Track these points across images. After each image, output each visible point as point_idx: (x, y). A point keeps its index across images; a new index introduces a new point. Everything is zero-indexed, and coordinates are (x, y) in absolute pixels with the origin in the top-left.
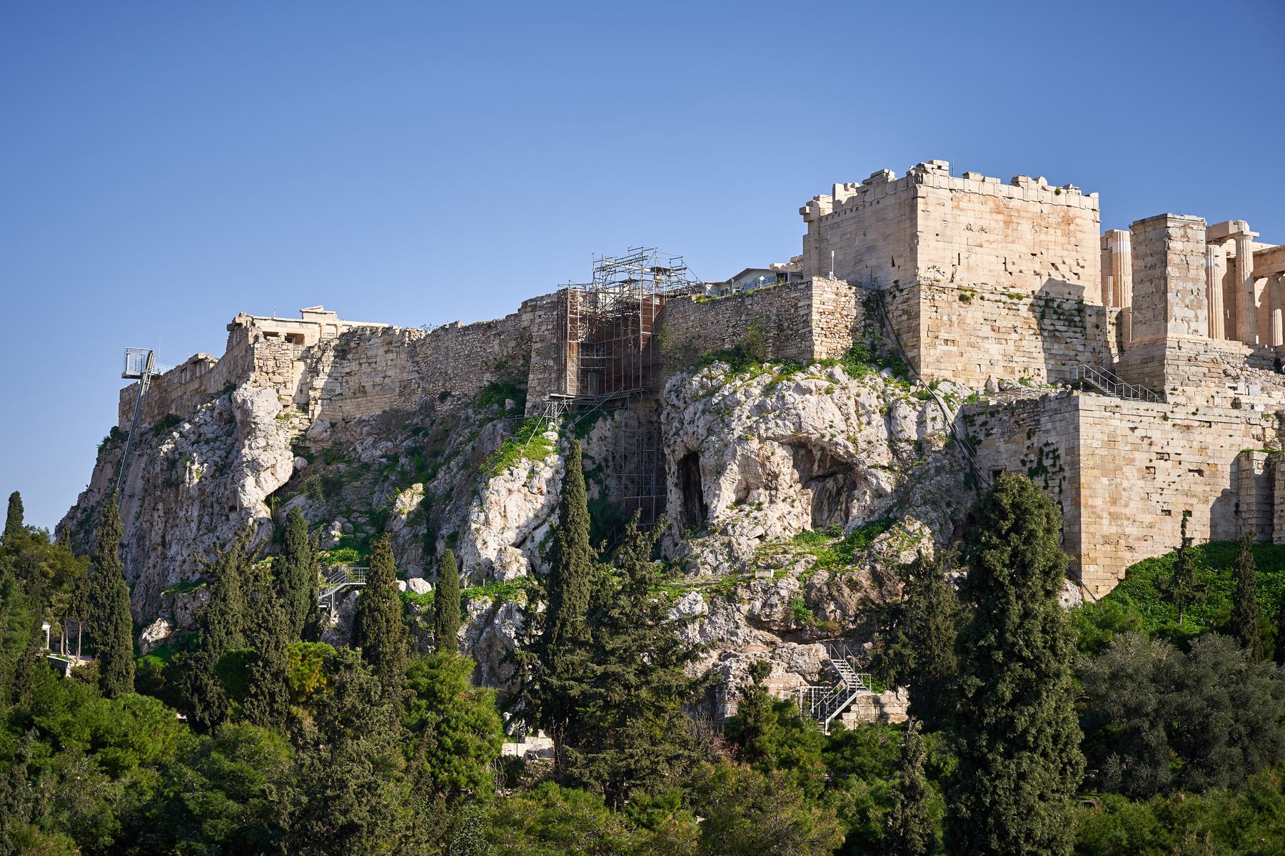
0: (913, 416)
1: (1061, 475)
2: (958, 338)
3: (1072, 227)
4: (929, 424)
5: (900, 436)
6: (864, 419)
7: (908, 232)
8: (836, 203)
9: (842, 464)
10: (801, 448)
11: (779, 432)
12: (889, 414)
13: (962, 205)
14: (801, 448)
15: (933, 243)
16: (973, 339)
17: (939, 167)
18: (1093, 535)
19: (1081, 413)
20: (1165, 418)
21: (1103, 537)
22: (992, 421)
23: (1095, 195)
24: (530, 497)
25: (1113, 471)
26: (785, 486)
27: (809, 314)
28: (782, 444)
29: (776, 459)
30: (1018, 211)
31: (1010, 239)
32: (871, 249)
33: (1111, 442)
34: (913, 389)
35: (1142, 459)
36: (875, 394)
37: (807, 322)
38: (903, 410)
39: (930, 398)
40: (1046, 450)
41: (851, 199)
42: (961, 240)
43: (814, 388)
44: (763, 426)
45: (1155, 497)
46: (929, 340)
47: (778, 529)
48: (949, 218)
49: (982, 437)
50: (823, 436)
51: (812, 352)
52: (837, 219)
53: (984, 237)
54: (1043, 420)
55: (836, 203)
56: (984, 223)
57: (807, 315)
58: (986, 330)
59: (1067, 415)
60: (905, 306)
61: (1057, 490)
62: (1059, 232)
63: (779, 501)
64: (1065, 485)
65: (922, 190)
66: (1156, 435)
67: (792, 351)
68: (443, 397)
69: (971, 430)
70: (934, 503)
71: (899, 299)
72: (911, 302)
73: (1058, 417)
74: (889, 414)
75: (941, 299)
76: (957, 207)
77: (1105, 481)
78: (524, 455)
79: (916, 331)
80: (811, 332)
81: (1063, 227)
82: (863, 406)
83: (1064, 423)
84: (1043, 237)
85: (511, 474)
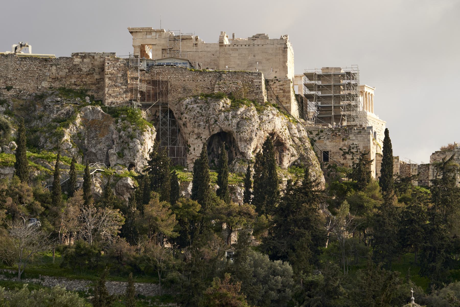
5: (295, 135)
7: (282, 60)
22: (321, 134)
40: (352, 146)
49: (316, 139)
59: (364, 135)
60: (281, 87)
73: (359, 136)
83: (361, 138)
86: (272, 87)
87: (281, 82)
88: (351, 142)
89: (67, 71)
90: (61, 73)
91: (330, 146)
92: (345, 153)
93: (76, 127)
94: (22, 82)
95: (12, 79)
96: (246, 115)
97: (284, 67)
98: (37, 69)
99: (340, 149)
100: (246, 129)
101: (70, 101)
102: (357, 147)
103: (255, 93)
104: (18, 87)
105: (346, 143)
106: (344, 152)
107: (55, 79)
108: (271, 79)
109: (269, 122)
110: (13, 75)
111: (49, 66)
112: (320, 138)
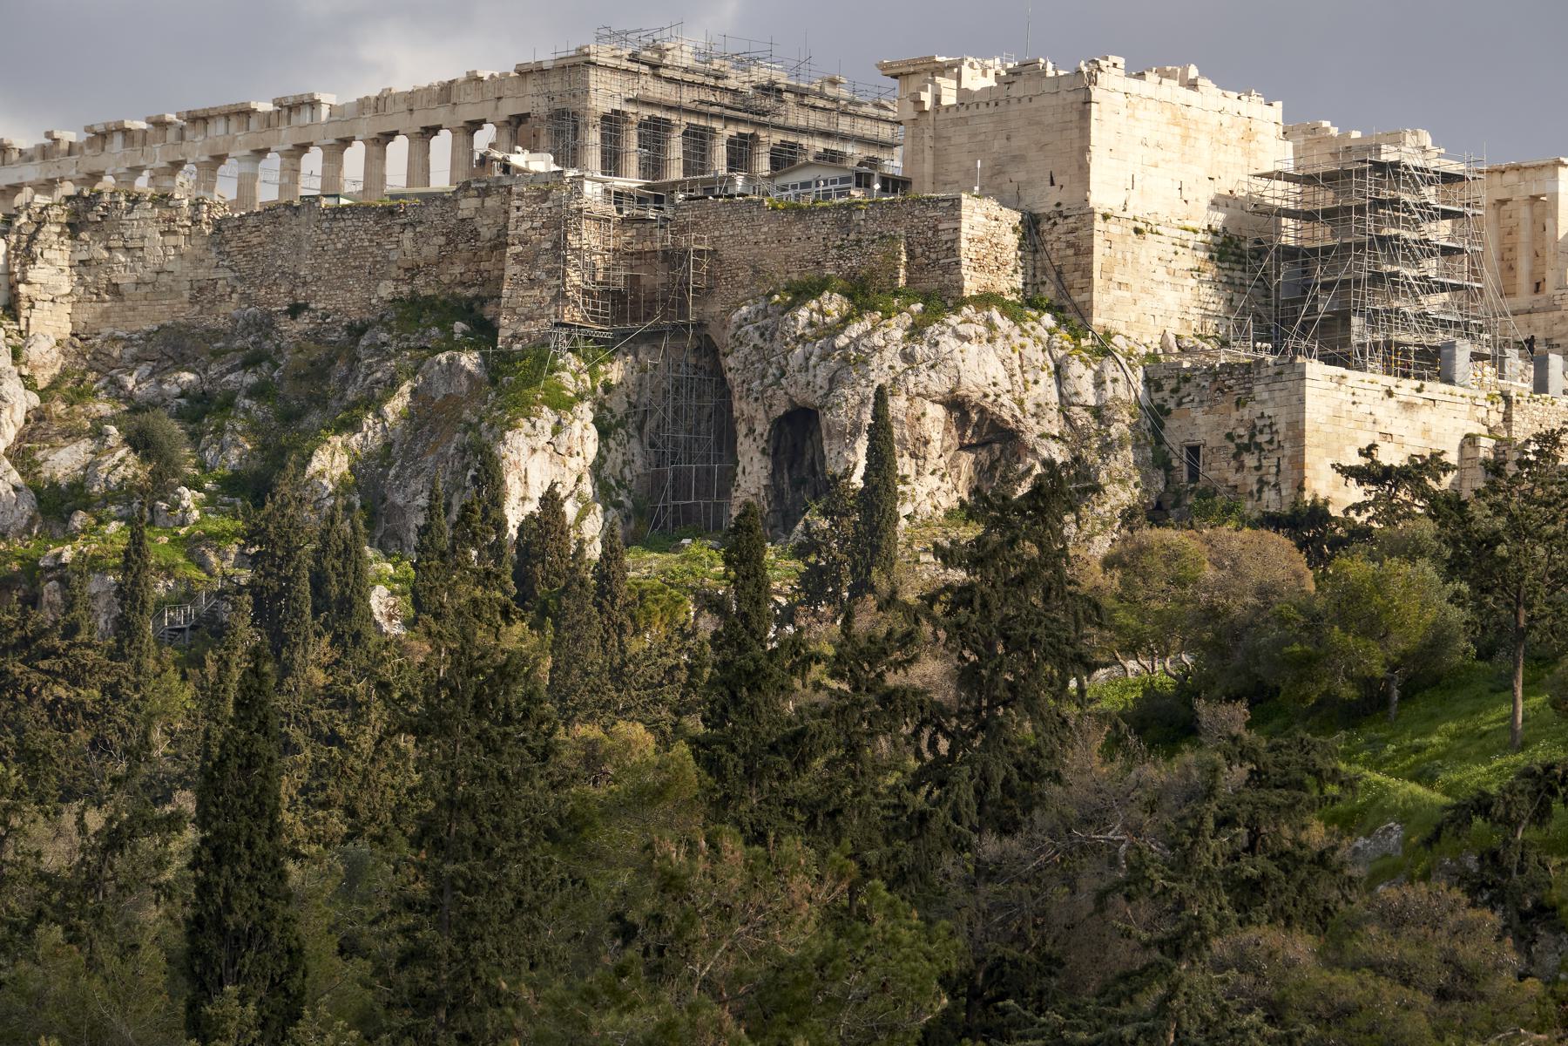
1: (1279, 454)
2: (1131, 282)
3: (1253, 145)
5: (1074, 399)
7: (1076, 145)
9: (1003, 430)
10: (956, 405)
12: (1059, 373)
13: (1138, 113)
14: (956, 405)
16: (1147, 283)
20: (1390, 394)
22: (1186, 388)
23: (1278, 105)
24: (557, 458)
26: (935, 455)
27: (956, 240)
29: (926, 421)
30: (1196, 122)
32: (1018, 159)
34: (1084, 343)
37: (953, 249)
38: (1076, 368)
39: (1107, 353)
40: (1259, 423)
44: (912, 379)
47: (927, 507)
49: (1171, 405)
50: (986, 396)
51: (961, 289)
52: (963, 113)
54: (1257, 389)
55: (963, 93)
57: (953, 241)
58: (1161, 274)
59: (1290, 384)
60: (1071, 237)
61: (1273, 470)
62: (1239, 151)
63: (927, 473)
64: (1284, 464)
65: (1096, 93)
66: (1380, 413)
67: (930, 285)
68: (295, 310)
69: (1157, 397)
70: (1121, 481)
73: (1278, 386)
74: (1059, 373)
75: (1114, 228)
76: (1133, 116)
78: (544, 402)
79: (1087, 273)
80: (958, 263)
83: (1284, 393)
85: (534, 426)
86: (1048, 238)
87: (1071, 220)
88: (1258, 409)
89: (442, 240)
90: (426, 250)
91: (1203, 429)
92: (1243, 449)
93: (384, 428)
94: (332, 288)
95: (309, 279)
96: (856, 349)
97: (1080, 167)
98: (371, 241)
99: (1229, 437)
100: (842, 394)
101: (407, 339)
102: (1271, 425)
103: (941, 268)
104: (321, 305)
105: (1245, 412)
106: (1238, 446)
107: (412, 271)
108: (1046, 210)
109: (933, 367)
110: (313, 268)
111: (397, 229)
112: (1179, 404)
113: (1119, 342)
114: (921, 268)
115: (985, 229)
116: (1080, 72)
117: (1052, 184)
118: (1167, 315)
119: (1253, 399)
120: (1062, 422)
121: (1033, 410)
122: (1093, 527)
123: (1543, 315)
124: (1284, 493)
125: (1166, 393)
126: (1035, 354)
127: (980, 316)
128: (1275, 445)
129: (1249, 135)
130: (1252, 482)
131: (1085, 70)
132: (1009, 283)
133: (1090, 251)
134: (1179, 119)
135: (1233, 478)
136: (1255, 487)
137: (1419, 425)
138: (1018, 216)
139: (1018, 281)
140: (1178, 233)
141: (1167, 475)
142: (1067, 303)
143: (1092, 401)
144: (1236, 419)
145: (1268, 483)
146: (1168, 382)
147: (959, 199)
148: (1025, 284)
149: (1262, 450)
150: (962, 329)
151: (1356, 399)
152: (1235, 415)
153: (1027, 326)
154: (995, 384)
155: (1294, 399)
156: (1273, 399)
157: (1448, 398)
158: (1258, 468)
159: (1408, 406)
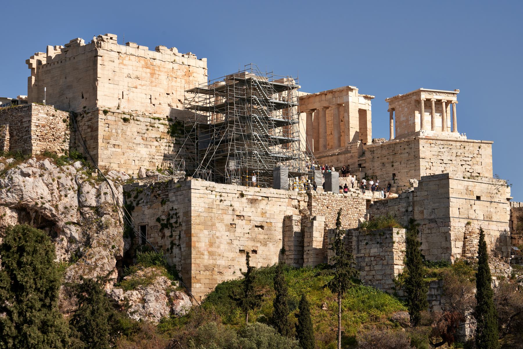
0: (93, 191)
1: (180, 229)
2: (121, 144)
3: (191, 78)
4: (103, 196)
6: (63, 193)
8: (49, 58)
11: (9, 200)
13: (125, 62)
15: (107, 85)
16: (131, 145)
17: (111, 38)
18: (199, 265)
19: (192, 191)
20: (242, 195)
21: (205, 266)
23: (205, 60)
25: (210, 226)
27: (30, 126)
28: (10, 208)
30: (159, 67)
31: (154, 84)
32: (69, 87)
33: (210, 209)
35: (228, 219)
36: (70, 177)
37: (28, 131)
38: (87, 187)
40: (171, 213)
41: (57, 56)
42: (124, 84)
43: (31, 173)
45: (236, 242)
46: (103, 145)
48: (117, 69)
49: (134, 204)
53: (139, 82)
54: (171, 195)
55: (49, 58)
56: (138, 74)
58: (139, 139)
59: (184, 192)
60: (89, 123)
61: (177, 237)
62: (183, 81)
65: (100, 52)
70: (105, 246)
71: (85, 119)
72: (93, 121)
76: (122, 63)
77: (206, 232)
79: (95, 139)
80: (30, 138)
81: (186, 78)
82: (63, 186)
83: (182, 197)
84: (173, 84)
86: (81, 124)
87: (90, 114)
91: (147, 216)
92: (164, 226)
102: (176, 214)
105: (165, 207)
106: (162, 225)
113: (112, 174)
114: (16, 142)
115: (47, 121)
116: (93, 42)
117: (83, 98)
118: (141, 160)
119: (169, 201)
120: (79, 216)
121: (63, 210)
122: (84, 272)
123: (343, 156)
124: (182, 250)
125: (132, 199)
126: (67, 182)
127: (38, 164)
128: (178, 225)
129: (188, 74)
130: (167, 243)
131: (95, 40)
132: (61, 147)
133: (97, 129)
134: (149, 65)
135: (160, 242)
136: (170, 246)
137: (259, 210)
138: (66, 114)
139: (66, 146)
140: (149, 120)
141: (132, 240)
142: (87, 155)
143: (94, 204)
144: (160, 211)
145: (175, 244)
146: (135, 194)
147: (31, 106)
148: (70, 148)
149: (172, 227)
150: (25, 170)
151: (222, 198)
152: (161, 209)
153: (64, 168)
154: (42, 198)
155: (186, 201)
156: (177, 200)
157: (276, 196)
158: (171, 236)
159: (253, 201)
